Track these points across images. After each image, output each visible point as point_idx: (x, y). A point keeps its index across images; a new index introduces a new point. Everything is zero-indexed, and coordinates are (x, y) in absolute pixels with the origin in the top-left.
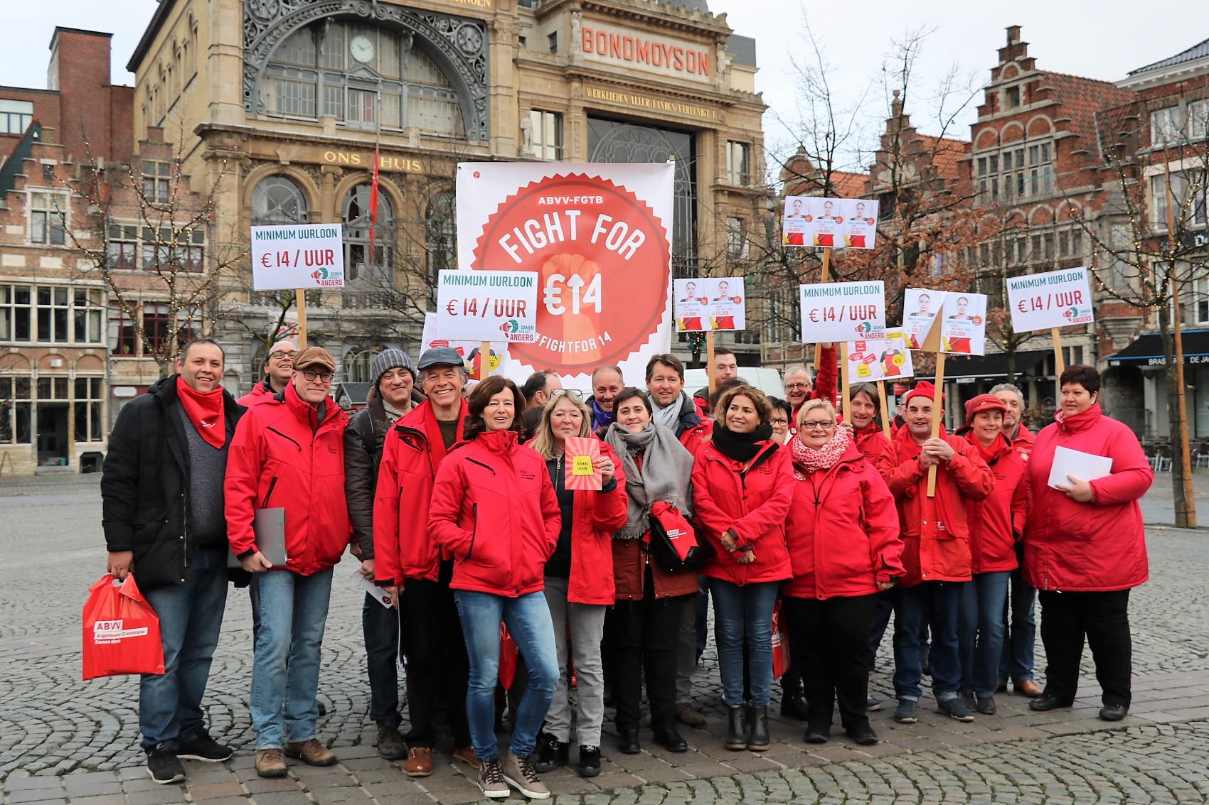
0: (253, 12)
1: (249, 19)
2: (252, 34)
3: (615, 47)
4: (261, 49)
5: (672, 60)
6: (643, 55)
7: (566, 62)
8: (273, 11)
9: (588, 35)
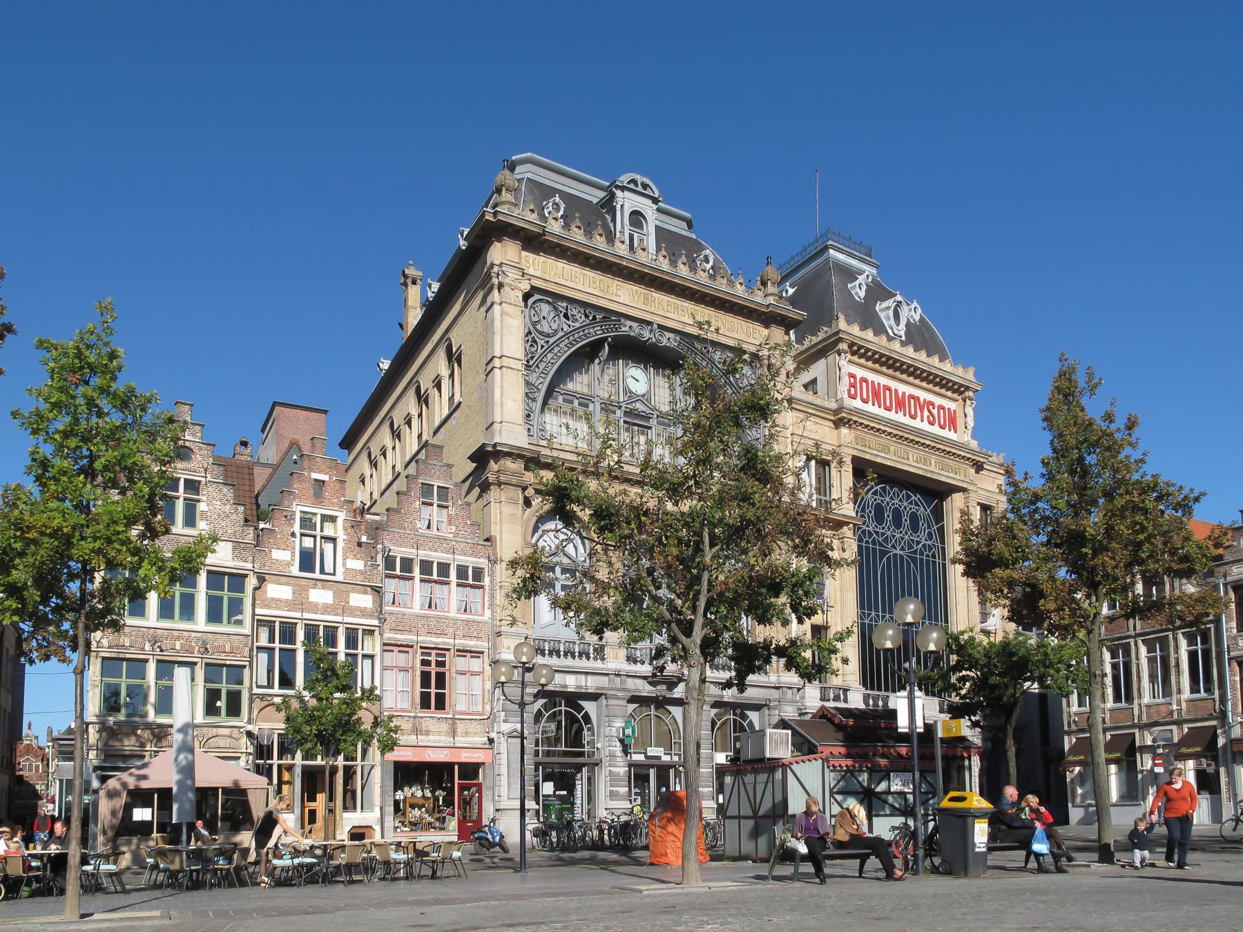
0: (534, 324)
1: (530, 333)
2: (533, 349)
3: (876, 394)
4: (542, 366)
5: (926, 413)
6: (900, 404)
7: (834, 406)
8: (555, 326)
9: (852, 380)
